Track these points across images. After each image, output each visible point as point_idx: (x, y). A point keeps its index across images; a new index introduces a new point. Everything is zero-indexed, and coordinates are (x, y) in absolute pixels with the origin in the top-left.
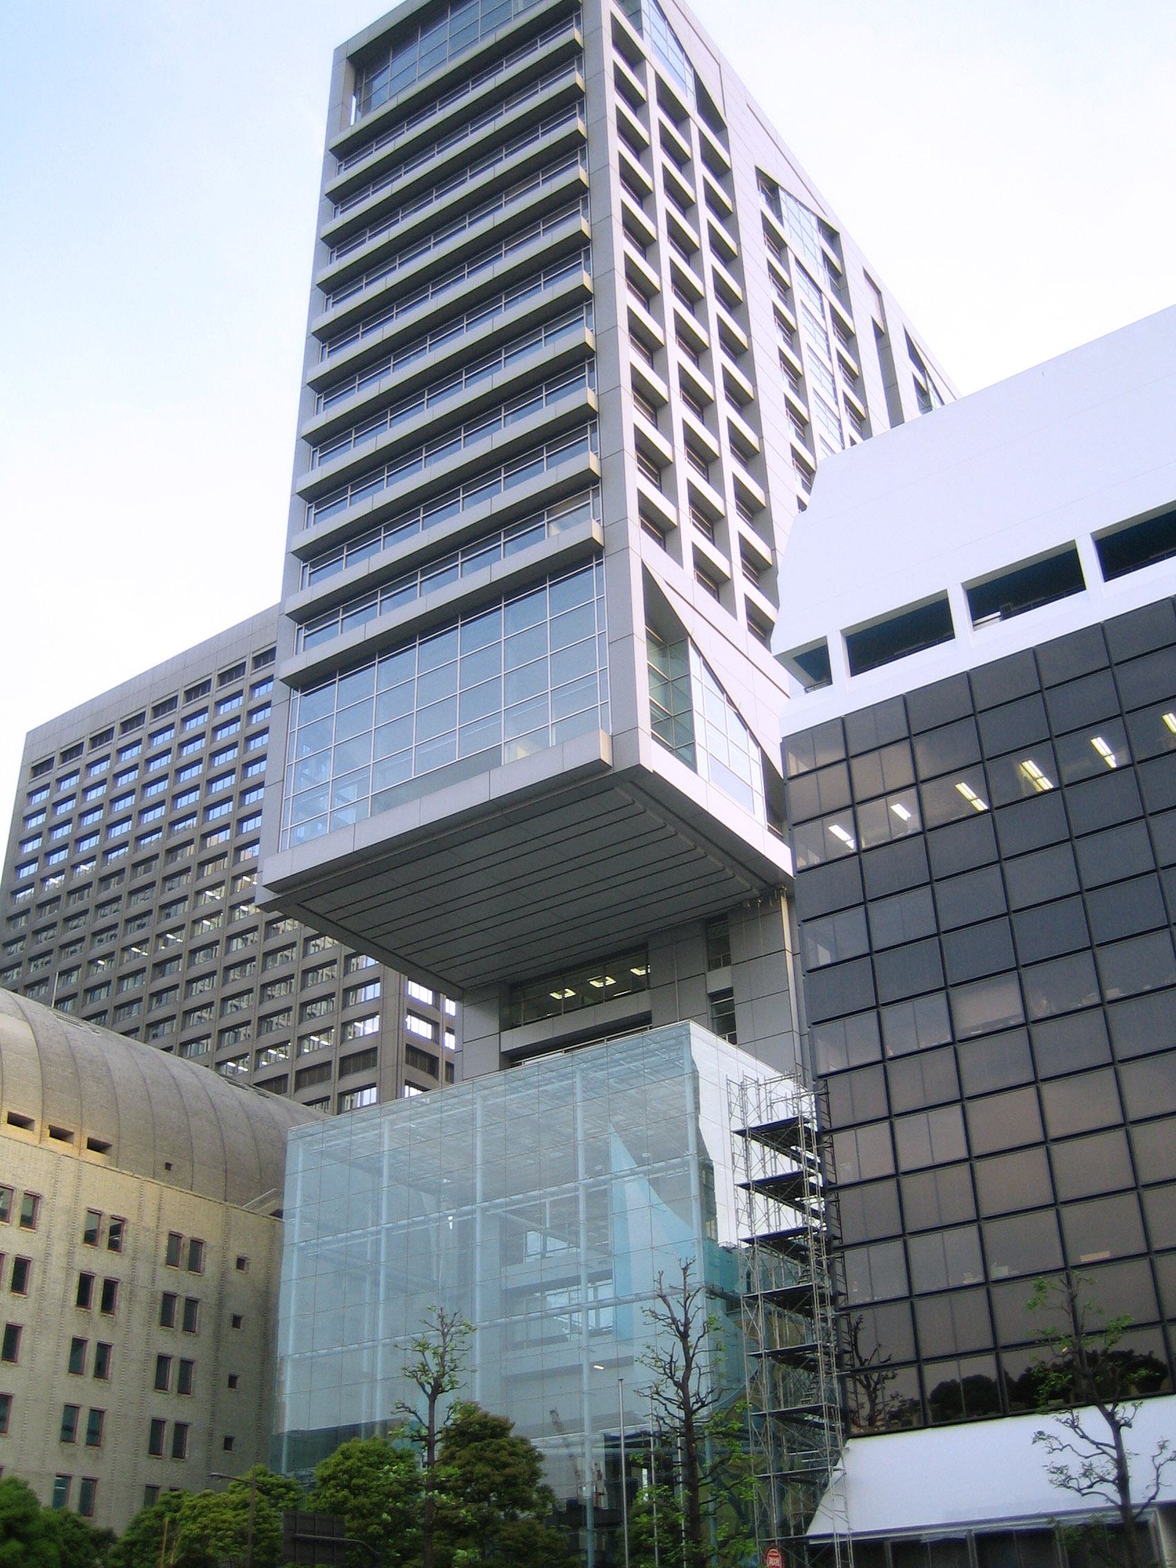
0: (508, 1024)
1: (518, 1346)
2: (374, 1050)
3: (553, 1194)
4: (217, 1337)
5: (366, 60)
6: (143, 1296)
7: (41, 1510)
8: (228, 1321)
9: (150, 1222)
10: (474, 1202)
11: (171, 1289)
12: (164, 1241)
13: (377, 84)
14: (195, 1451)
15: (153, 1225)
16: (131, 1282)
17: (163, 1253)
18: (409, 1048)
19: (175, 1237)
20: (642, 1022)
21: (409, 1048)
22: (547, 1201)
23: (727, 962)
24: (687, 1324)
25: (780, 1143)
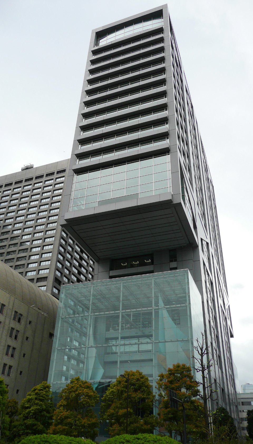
0: (111, 269)
1: (109, 354)
2: (47, 277)
3: (133, 312)
4: (22, 343)
5: (100, 35)
6: (6, 327)
7: (239, 390)
8: (25, 339)
9: (11, 307)
10: (119, 310)
11: (13, 327)
12: (13, 313)
13: (101, 41)
14: (12, 374)
15: (11, 308)
16: (4, 323)
17: (13, 317)
18: (56, 278)
19: (16, 312)
20: (152, 272)
21: (56, 278)
22: (132, 313)
23: (176, 261)
24: (203, 348)
25: (140, 314)
